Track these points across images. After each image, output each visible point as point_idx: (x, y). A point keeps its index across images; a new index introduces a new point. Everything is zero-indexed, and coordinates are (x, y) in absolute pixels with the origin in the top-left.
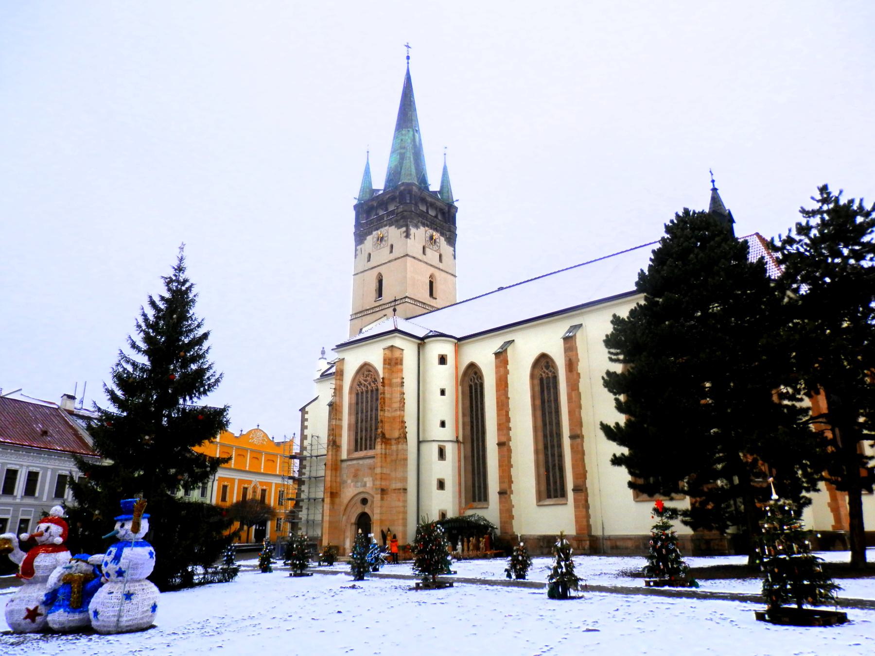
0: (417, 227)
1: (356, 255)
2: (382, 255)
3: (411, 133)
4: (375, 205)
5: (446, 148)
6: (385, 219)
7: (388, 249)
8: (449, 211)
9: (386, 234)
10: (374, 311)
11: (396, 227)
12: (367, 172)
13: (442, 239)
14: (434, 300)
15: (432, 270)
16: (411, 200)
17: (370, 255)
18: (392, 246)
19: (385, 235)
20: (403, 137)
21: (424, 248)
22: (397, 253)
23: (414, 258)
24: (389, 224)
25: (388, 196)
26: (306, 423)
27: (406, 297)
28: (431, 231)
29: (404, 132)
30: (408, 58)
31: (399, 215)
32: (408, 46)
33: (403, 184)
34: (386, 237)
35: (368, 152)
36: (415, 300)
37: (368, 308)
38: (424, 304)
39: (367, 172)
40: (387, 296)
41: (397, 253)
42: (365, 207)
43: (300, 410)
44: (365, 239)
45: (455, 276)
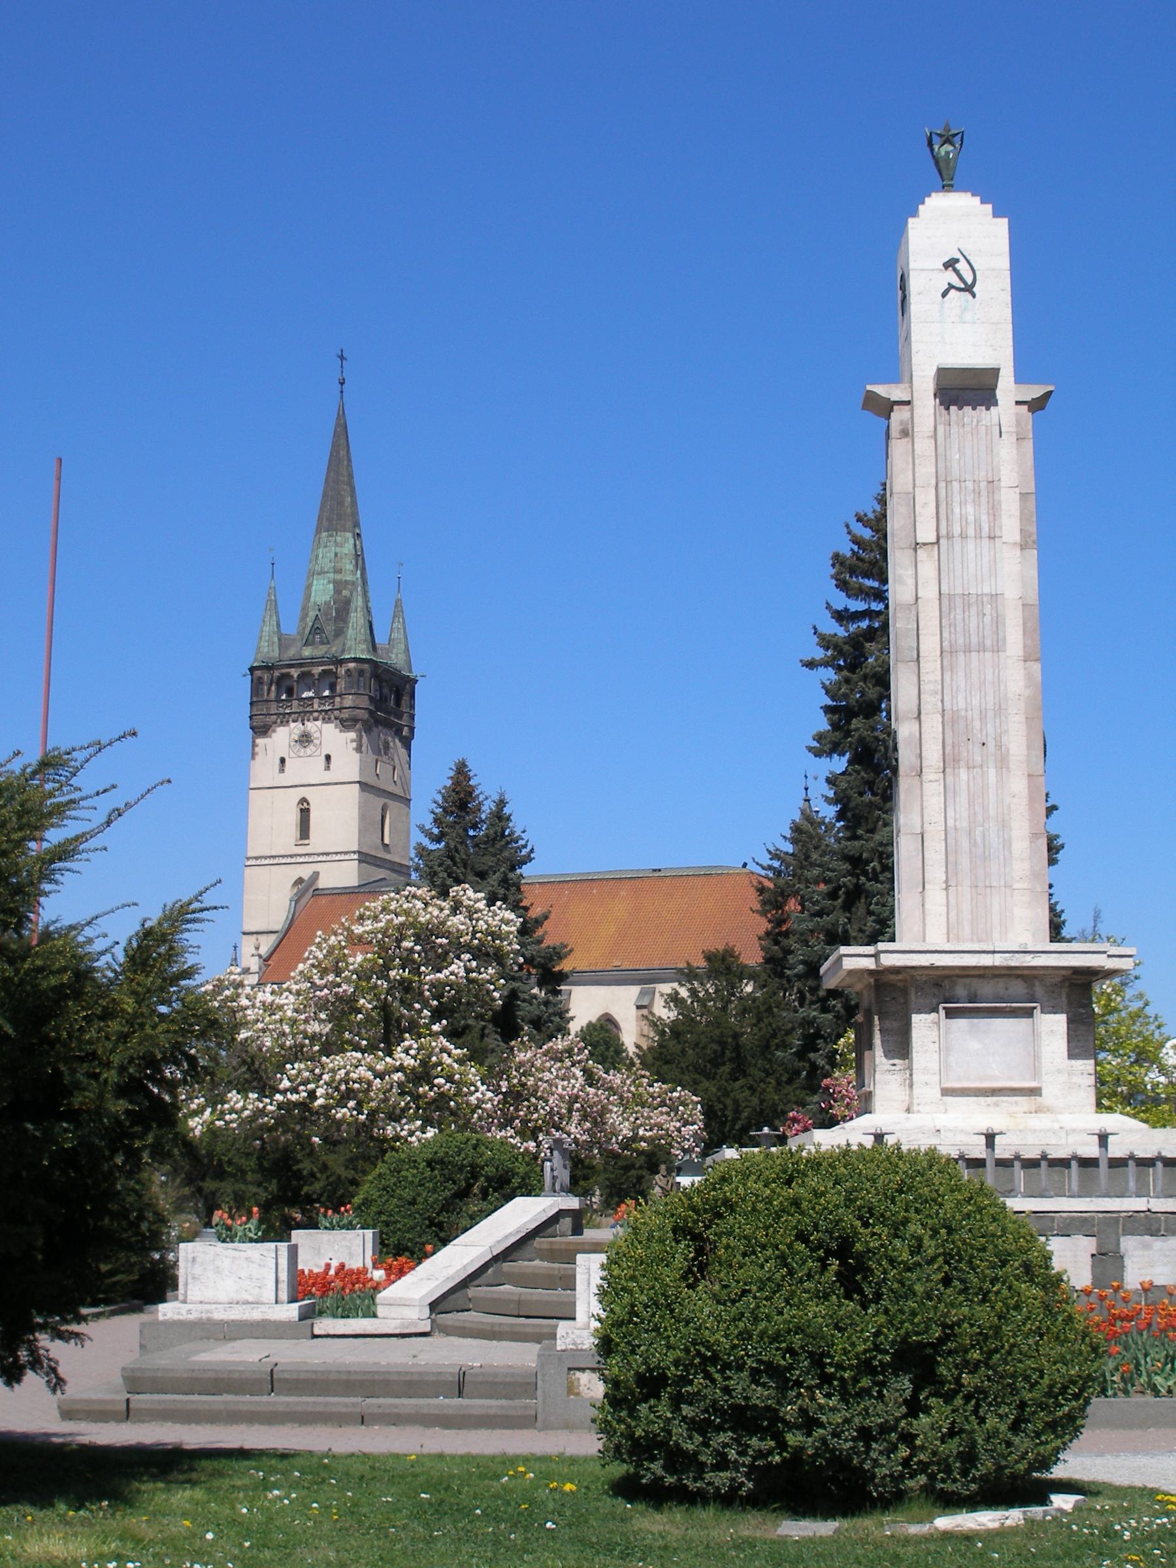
2: (305, 767)
3: (352, 541)
4: (295, 676)
6: (316, 707)
7: (323, 759)
10: (293, 860)
11: (336, 727)
17: (283, 760)
18: (328, 758)
20: (338, 549)
25: (321, 668)
27: (354, 852)
29: (339, 539)
30: (342, 384)
32: (342, 358)
33: (355, 660)
36: (367, 855)
37: (282, 853)
40: (319, 840)
44: (274, 731)
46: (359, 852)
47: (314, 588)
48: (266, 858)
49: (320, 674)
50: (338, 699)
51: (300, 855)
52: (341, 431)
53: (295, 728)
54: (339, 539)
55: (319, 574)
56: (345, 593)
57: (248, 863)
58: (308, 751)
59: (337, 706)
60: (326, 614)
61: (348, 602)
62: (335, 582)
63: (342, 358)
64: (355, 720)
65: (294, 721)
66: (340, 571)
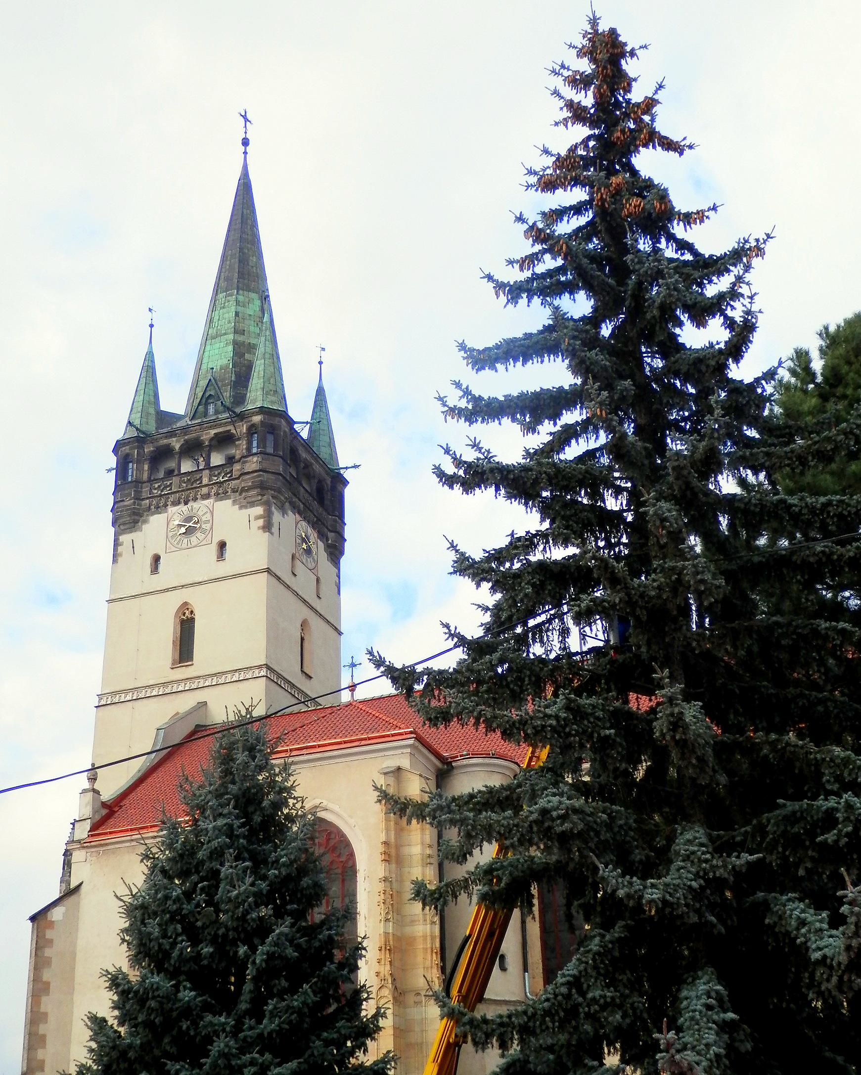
0: (282, 509)
1: (116, 556)
3: (258, 303)
4: (177, 447)
5: (323, 349)
6: (205, 481)
7: (214, 549)
8: (334, 488)
9: (208, 516)
10: (167, 691)
11: (234, 502)
12: (149, 371)
13: (321, 545)
14: (308, 681)
15: (306, 613)
16: (275, 448)
17: (157, 559)
18: (222, 545)
19: (204, 519)
20: (240, 309)
21: (293, 557)
22: (233, 564)
23: (279, 579)
24: (217, 494)
25: (213, 432)
26: (48, 952)
27: (260, 667)
28: (304, 523)
30: (245, 142)
31: (248, 477)
32: (246, 120)
33: (262, 410)
34: (207, 522)
35: (151, 326)
36: (279, 676)
37: (151, 682)
38: (293, 686)
39: (149, 371)
41: (234, 561)
42: (148, 449)
43: (33, 919)
44: (145, 522)
45: (340, 633)
46: (268, 668)
47: (206, 354)
48: (126, 691)
49: (211, 440)
50: (237, 467)
51: (178, 682)
52: (245, 190)
53: (176, 513)
54: (241, 298)
55: (213, 338)
56: (247, 356)
57: (103, 703)
58: (194, 540)
59: (236, 474)
60: (223, 380)
61: (250, 367)
62: (235, 343)
63: (245, 117)
64: (262, 487)
65: (176, 503)
66: (243, 332)
